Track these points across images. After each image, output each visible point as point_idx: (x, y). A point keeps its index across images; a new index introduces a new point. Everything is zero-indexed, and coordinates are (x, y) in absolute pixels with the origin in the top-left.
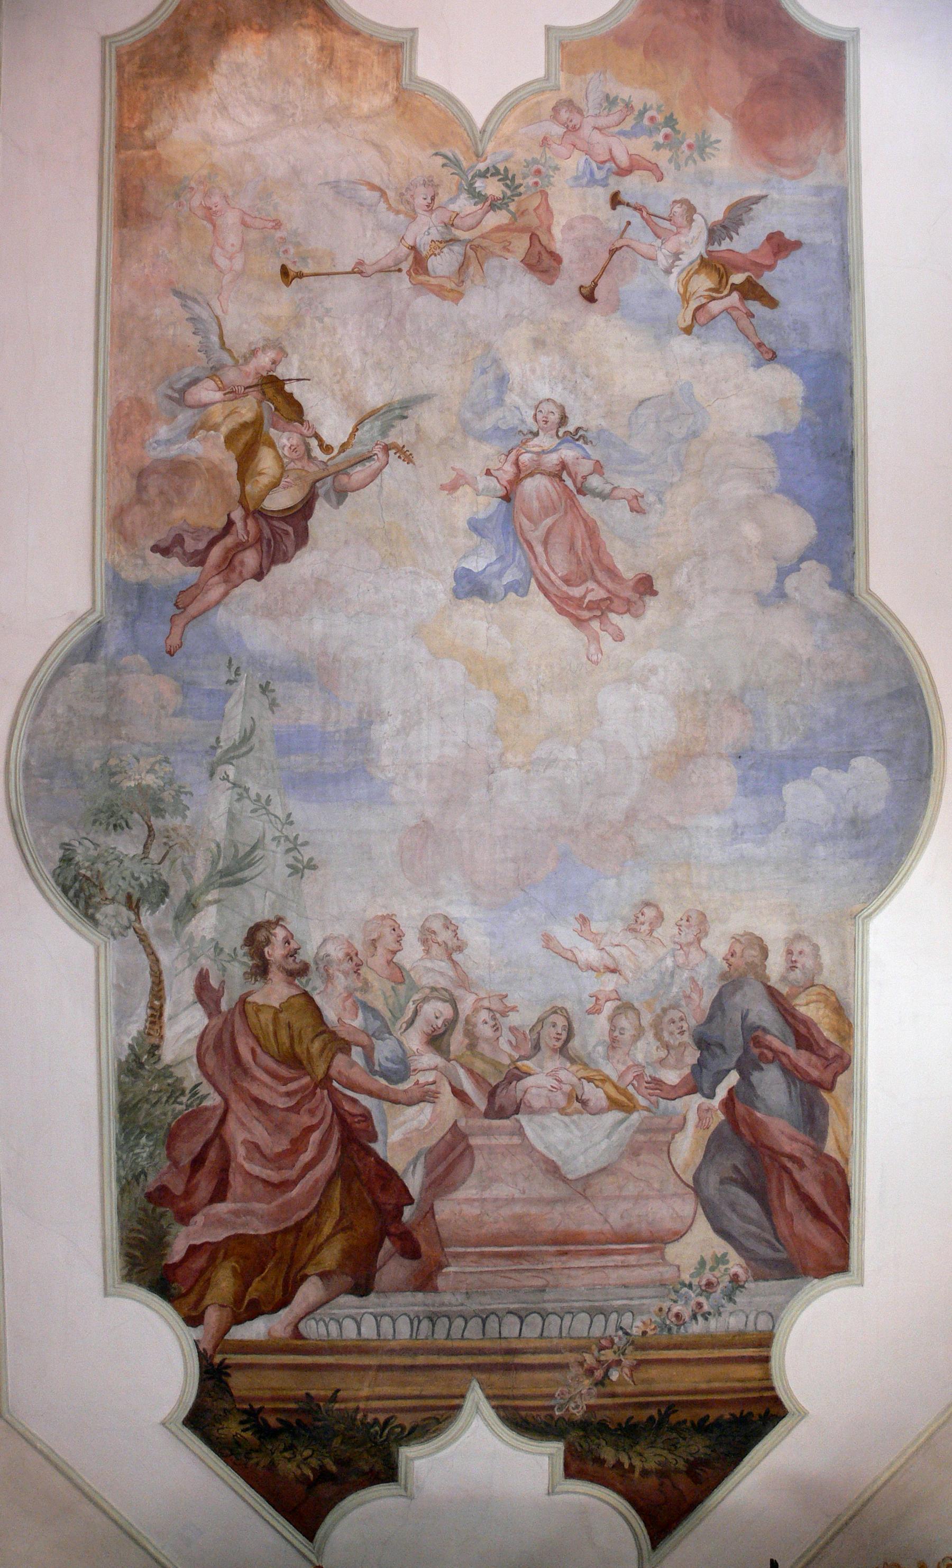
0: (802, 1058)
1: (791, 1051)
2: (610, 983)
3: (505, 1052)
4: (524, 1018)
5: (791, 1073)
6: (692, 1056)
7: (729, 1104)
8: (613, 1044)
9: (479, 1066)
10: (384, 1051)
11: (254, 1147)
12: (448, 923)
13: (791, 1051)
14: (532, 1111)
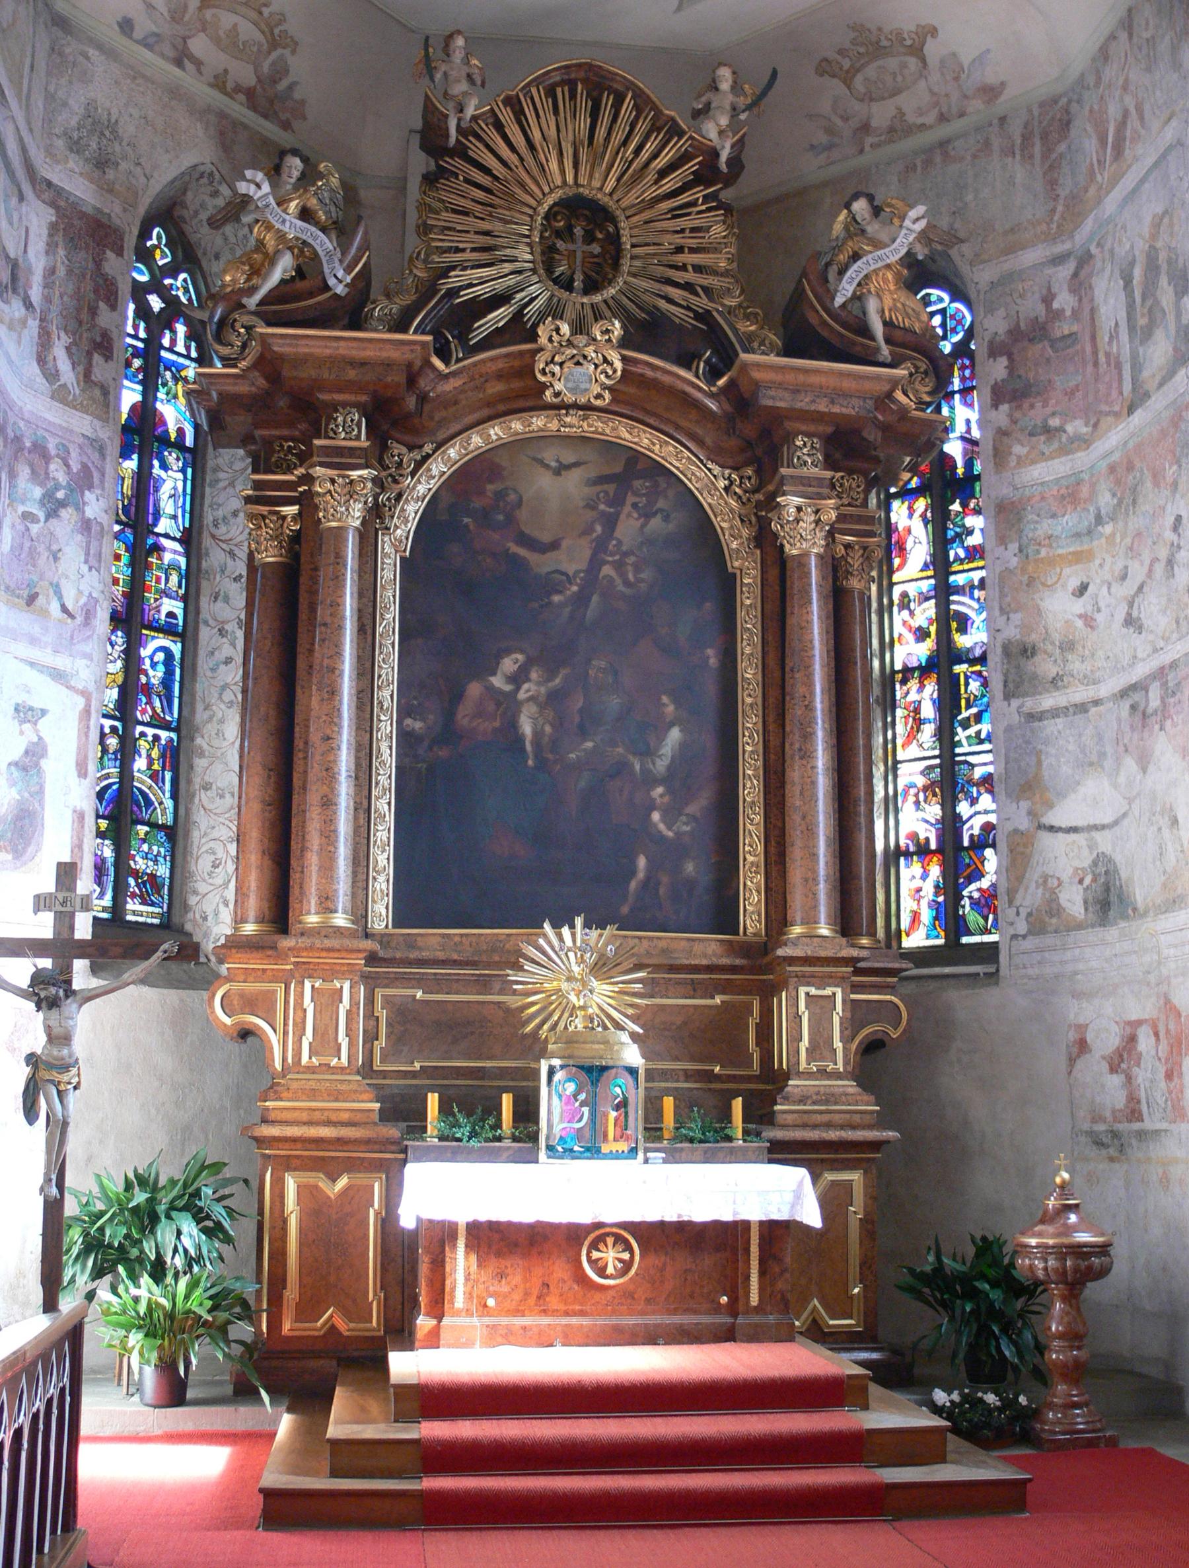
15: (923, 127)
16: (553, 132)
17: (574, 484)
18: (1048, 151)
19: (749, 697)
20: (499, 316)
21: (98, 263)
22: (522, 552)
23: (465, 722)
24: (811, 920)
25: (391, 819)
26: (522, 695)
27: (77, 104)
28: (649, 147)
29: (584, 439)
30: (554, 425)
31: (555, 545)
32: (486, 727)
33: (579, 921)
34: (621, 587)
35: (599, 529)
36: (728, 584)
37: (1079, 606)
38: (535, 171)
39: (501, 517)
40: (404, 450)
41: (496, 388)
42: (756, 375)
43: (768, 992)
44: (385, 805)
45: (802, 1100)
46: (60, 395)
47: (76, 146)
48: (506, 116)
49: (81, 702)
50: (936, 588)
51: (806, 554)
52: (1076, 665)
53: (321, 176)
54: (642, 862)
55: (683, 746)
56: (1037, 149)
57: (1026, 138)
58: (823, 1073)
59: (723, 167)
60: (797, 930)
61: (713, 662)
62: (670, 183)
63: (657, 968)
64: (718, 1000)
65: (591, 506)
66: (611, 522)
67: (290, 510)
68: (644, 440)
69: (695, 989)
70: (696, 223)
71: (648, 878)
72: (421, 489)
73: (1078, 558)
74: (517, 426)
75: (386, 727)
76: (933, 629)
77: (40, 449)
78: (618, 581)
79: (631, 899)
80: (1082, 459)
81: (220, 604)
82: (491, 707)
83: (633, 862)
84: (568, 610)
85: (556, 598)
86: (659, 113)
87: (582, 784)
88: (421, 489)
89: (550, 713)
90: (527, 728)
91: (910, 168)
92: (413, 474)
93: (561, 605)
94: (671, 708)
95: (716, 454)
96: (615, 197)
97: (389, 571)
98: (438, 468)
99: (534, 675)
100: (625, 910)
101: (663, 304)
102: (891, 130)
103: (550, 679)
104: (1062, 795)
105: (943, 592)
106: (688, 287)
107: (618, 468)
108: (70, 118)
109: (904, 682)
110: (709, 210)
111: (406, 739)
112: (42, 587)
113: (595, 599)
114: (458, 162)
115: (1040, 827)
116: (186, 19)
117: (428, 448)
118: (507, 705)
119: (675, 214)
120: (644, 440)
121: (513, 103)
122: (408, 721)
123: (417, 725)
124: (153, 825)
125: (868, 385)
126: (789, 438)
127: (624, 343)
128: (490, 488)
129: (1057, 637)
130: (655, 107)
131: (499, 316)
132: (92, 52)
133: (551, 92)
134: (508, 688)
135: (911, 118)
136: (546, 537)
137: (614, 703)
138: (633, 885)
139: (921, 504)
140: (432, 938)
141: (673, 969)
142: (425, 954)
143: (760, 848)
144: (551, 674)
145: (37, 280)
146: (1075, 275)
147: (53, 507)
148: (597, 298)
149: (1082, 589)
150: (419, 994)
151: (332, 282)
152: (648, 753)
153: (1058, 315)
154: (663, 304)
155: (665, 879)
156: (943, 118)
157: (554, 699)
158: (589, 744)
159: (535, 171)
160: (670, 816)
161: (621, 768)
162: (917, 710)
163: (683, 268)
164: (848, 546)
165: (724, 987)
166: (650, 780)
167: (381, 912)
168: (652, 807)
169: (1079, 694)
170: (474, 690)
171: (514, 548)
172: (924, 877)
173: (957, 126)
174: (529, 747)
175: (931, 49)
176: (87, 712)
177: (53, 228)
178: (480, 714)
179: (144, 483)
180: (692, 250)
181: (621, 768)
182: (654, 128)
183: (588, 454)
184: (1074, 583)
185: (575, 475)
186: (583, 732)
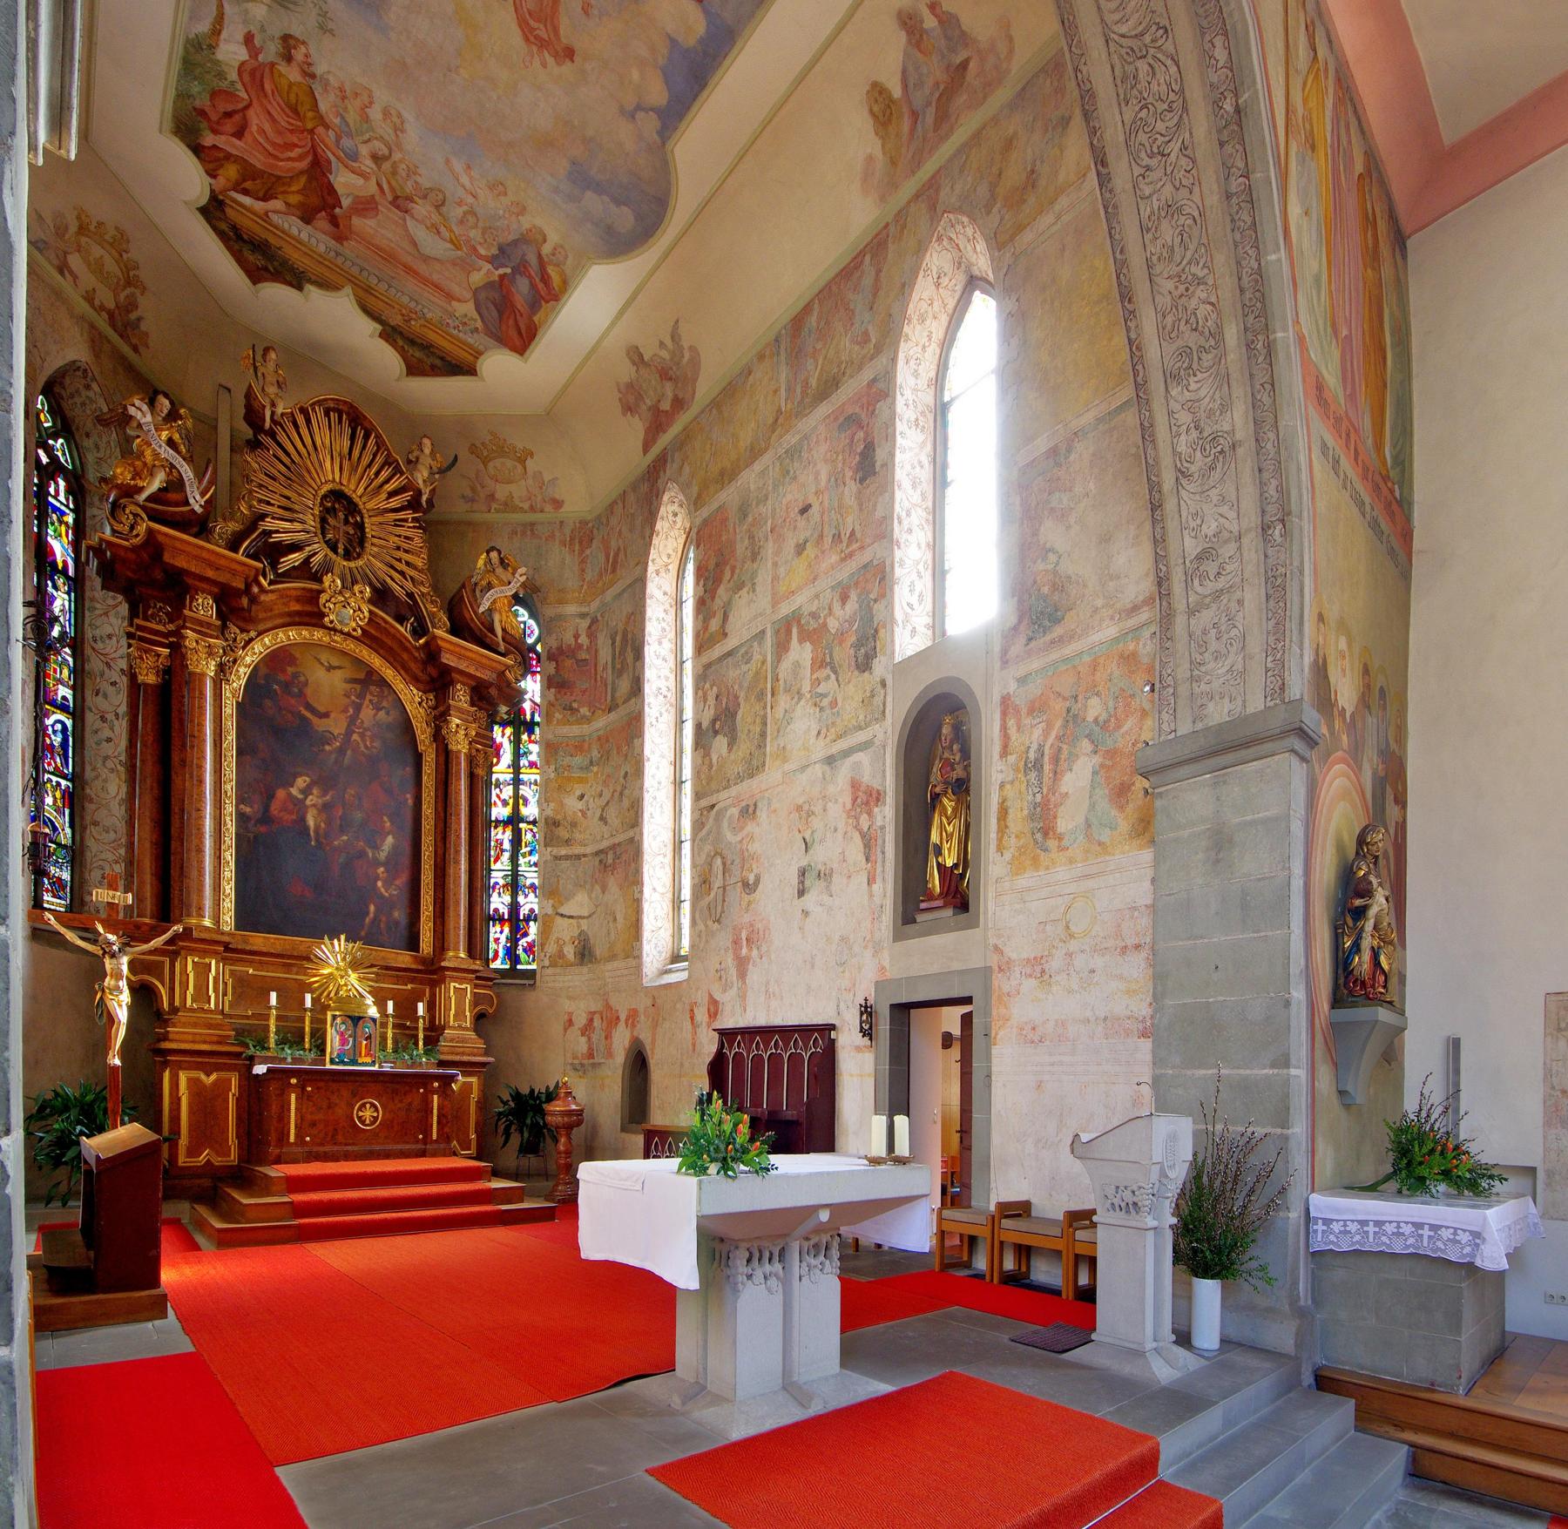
0: (541, 286)
1: (537, 280)
2: (470, 200)
3: (409, 188)
4: (426, 183)
5: (533, 286)
6: (495, 251)
7: (502, 277)
8: (461, 222)
9: (394, 183)
10: (346, 143)
11: (262, 131)
12: (399, 116)
13: (537, 280)
14: (412, 217)
18: (582, 551)
19: (428, 825)
20: (295, 558)
22: (308, 715)
23: (276, 812)
25: (232, 865)
26: (308, 802)
28: (384, 475)
30: (326, 639)
31: (326, 715)
32: (289, 818)
34: (363, 749)
35: (351, 710)
36: (418, 758)
37: (580, 805)
39: (296, 690)
40: (238, 631)
41: (296, 607)
43: (434, 984)
44: (229, 856)
48: (301, 419)
50: (513, 779)
51: (460, 751)
52: (577, 836)
53: (181, 418)
54: (372, 908)
56: (577, 548)
57: (572, 539)
60: (451, 954)
61: (410, 802)
62: (395, 502)
64: (409, 987)
65: (347, 696)
66: (358, 708)
67: (166, 651)
68: (376, 662)
69: (398, 980)
70: (408, 534)
72: (248, 660)
73: (581, 780)
75: (230, 808)
76: (511, 801)
78: (362, 745)
79: (366, 928)
80: (585, 729)
81: (100, 699)
83: (368, 907)
84: (333, 756)
85: (327, 748)
86: (389, 454)
87: (341, 860)
88: (248, 660)
90: (311, 822)
92: (244, 648)
93: (331, 752)
94: (388, 824)
95: (415, 680)
96: (364, 499)
97: (229, 709)
99: (315, 791)
100: (363, 934)
103: (324, 795)
104: (567, 899)
105: (517, 782)
106: (402, 573)
107: (362, 676)
109: (496, 827)
110: (414, 527)
111: (241, 818)
113: (349, 752)
114: (268, 440)
116: (67, 237)
117: (253, 634)
118: (299, 806)
119: (398, 523)
121: (303, 411)
122: (242, 806)
124: (59, 845)
126: (452, 683)
127: (371, 601)
128: (290, 670)
131: (295, 558)
134: (300, 796)
135: (517, 502)
136: (322, 709)
137: (358, 816)
138: (367, 920)
139: (509, 730)
140: (259, 941)
141: (387, 968)
142: (255, 948)
143: (431, 908)
144: (325, 793)
146: (589, 627)
148: (352, 564)
149: (582, 797)
150: (251, 971)
151: (192, 501)
152: (376, 848)
153: (580, 647)
155: (384, 919)
156: (532, 509)
157: (326, 808)
158: (345, 838)
160: (387, 884)
161: (362, 854)
162: (502, 844)
163: (399, 560)
164: (477, 750)
165: (412, 981)
168: (377, 878)
169: (577, 850)
170: (281, 794)
172: (501, 932)
174: (312, 833)
180: (406, 551)
183: (346, 663)
184: (578, 793)
185: (338, 676)
186: (342, 830)
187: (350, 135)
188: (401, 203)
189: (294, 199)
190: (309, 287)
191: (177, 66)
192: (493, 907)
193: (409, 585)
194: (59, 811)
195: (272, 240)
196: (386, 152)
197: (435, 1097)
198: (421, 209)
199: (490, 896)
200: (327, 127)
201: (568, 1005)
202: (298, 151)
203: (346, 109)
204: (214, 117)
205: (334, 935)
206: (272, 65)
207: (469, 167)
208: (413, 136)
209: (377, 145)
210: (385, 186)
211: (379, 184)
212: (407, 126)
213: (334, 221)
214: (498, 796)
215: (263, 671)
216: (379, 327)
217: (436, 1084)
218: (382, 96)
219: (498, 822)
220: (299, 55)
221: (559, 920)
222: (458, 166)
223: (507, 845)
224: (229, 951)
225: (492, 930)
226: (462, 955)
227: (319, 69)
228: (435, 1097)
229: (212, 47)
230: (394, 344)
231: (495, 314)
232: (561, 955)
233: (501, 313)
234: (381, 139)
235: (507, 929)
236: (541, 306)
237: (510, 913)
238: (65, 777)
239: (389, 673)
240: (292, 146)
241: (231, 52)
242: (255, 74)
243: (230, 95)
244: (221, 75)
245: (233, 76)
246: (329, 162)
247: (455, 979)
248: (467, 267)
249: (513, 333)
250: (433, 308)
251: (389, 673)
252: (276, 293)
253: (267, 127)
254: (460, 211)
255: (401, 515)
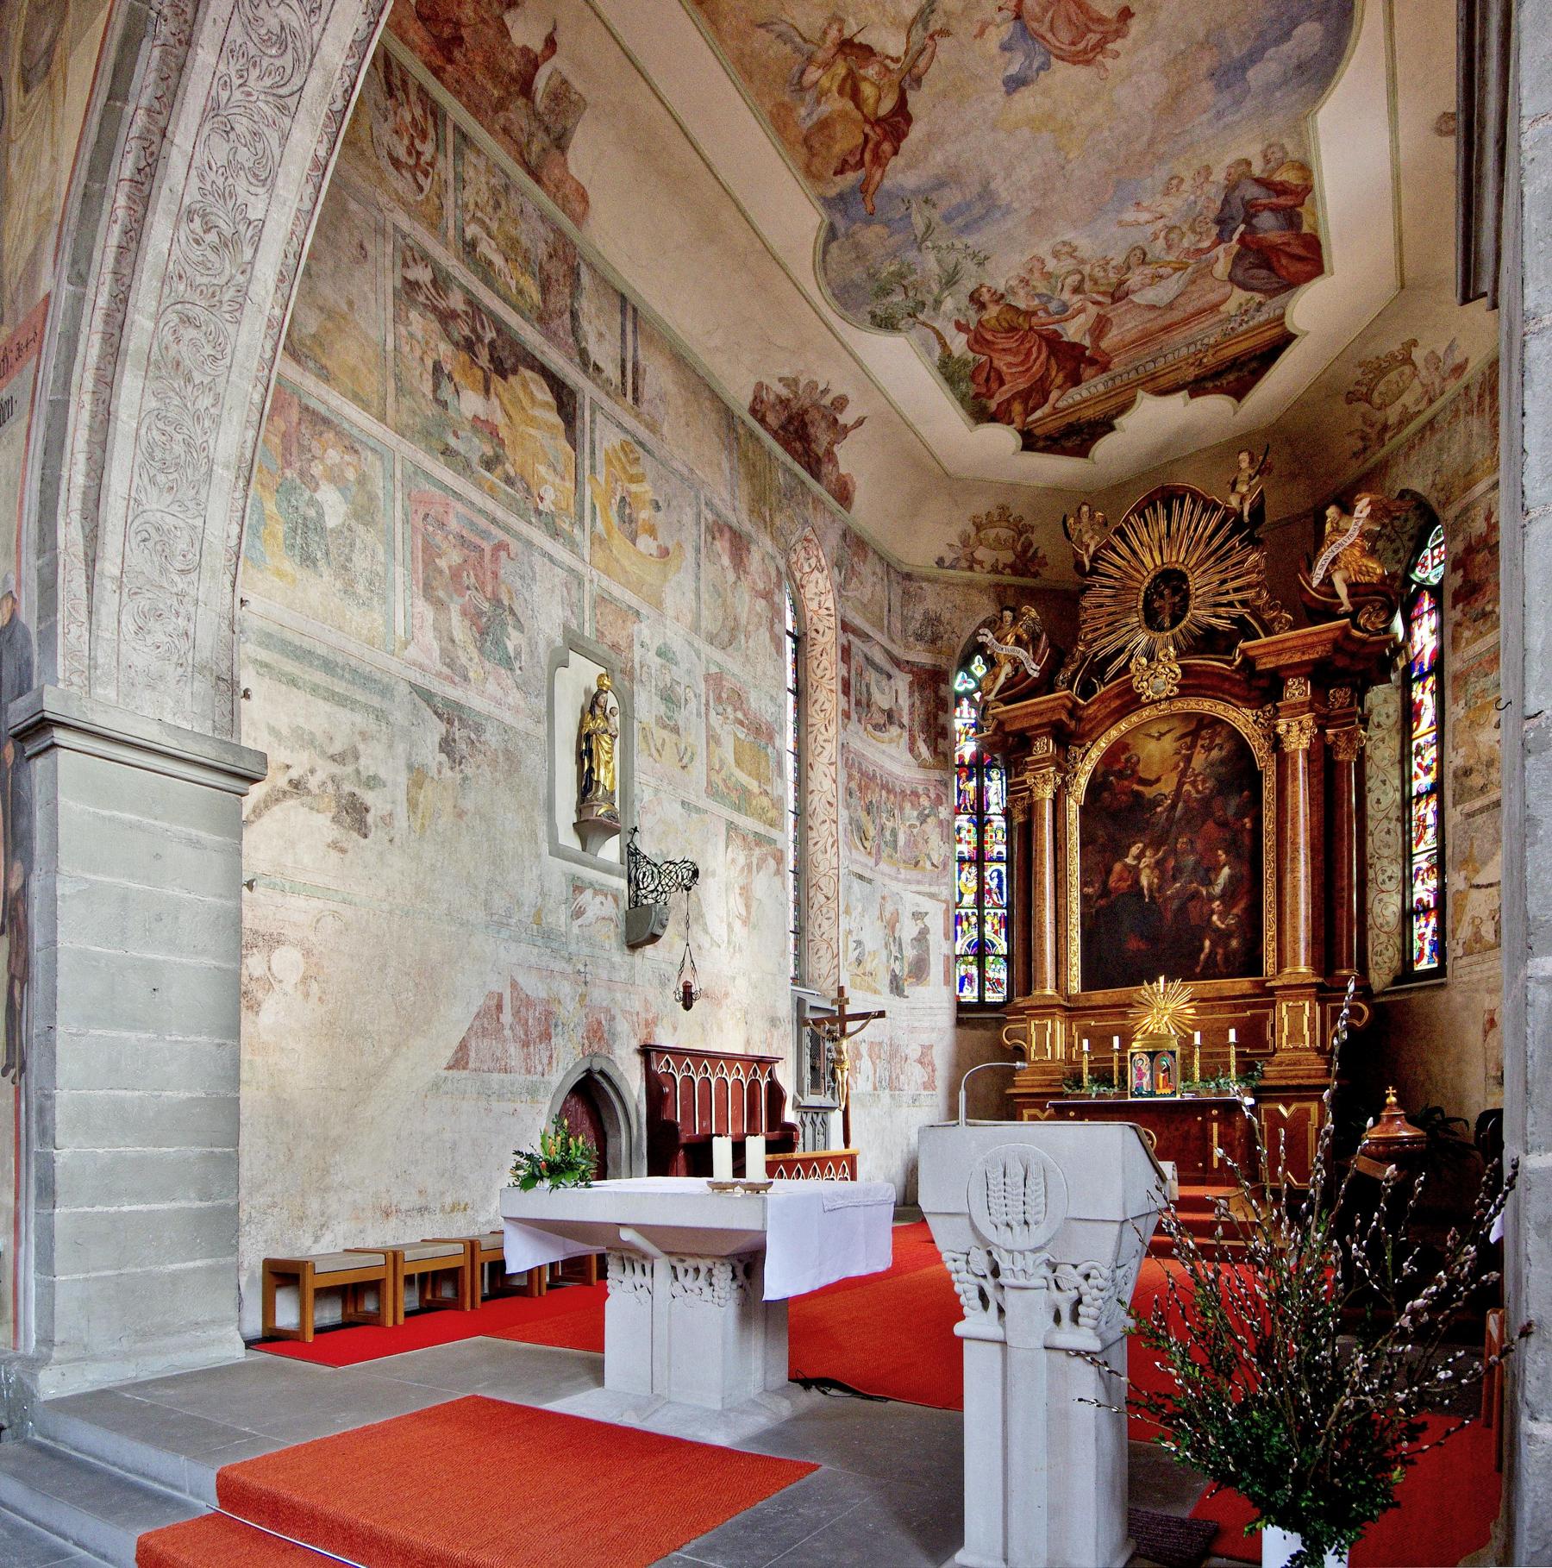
0: (1282, 201)
1: (1274, 200)
2: (1160, 224)
3: (1113, 277)
4: (1119, 260)
5: (1274, 209)
6: (1215, 230)
7: (1241, 240)
8: (1169, 247)
9: (1102, 289)
10: (1053, 307)
11: (1010, 365)
12: (1064, 243)
13: (1274, 200)
14: (1134, 292)
15: (1419, 412)
16: (1146, 538)
17: (1168, 743)
19: (1268, 842)
21: (936, 692)
22: (1140, 788)
24: (1296, 964)
27: (918, 616)
29: (1173, 716)
31: (1158, 780)
32: (1124, 885)
33: (1162, 979)
34: (1194, 795)
37: (1497, 735)
38: (1138, 566)
42: (1251, 653)
45: (1280, 1064)
46: (923, 765)
47: (919, 637)
49: (944, 906)
54: (1207, 943)
55: (1231, 877)
58: (1296, 1048)
59: (1246, 519)
60: (1287, 970)
62: (1216, 542)
63: (1203, 1000)
65: (1177, 753)
66: (1188, 759)
68: (1206, 706)
69: (1237, 1008)
71: (1211, 951)
74: (1134, 719)
77: (915, 794)
82: (1125, 875)
88: (1088, 768)
89: (1157, 872)
90: (1144, 882)
91: (1412, 447)
98: (1095, 754)
100: (1198, 970)
101: (1213, 621)
102: (1401, 422)
104: (1484, 863)
106: (1231, 604)
107: (1192, 727)
108: (914, 626)
111: (1085, 898)
112: (922, 857)
115: (1472, 886)
117: (1089, 744)
118: (1135, 872)
119: (1221, 559)
120: (1206, 706)
123: (1089, 890)
125: (1324, 636)
128: (1123, 758)
129: (1484, 758)
130: (1203, 498)
132: (924, 584)
133: (1142, 515)
136: (1153, 777)
141: (1222, 999)
145: (906, 712)
147: (923, 819)
154: (1213, 621)
155: (1220, 951)
156: (1431, 401)
157: (1159, 865)
159: (1138, 566)
160: (1223, 917)
166: (1211, 899)
167: (1075, 985)
168: (1213, 912)
170: (1118, 867)
171: (1136, 787)
173: (1437, 405)
175: (1418, 355)
176: (947, 910)
177: (911, 683)
178: (1121, 879)
179: (980, 791)
181: (1195, 895)
182: (1205, 510)
183: (1175, 723)
184: (1494, 721)
185: (1169, 736)
186: (1175, 879)
187: (1050, 299)
188: (1118, 294)
189: (1059, 380)
190: (1116, 422)
191: (946, 387)
192: (1415, 898)
193: (1240, 610)
194: (996, 932)
195: (1072, 419)
196: (1077, 277)
197: (1215, 1125)
198: (1134, 279)
199: (1412, 886)
200: (1034, 313)
201: (1488, 1002)
202: (1035, 349)
203: (1034, 287)
204: (984, 390)
205: (1152, 979)
206: (980, 322)
207: (1138, 204)
208: (1086, 245)
209: (1073, 280)
210: (1100, 298)
211: (1094, 303)
212: (1075, 243)
213: (1092, 362)
214: (1419, 765)
215: (1101, 769)
216: (1185, 393)
217: (1215, 1112)
218: (1043, 249)
219: (1419, 796)
220: (986, 297)
221: (1474, 893)
222: (1129, 216)
223: (1431, 819)
224: (1072, 1010)
225: (1416, 925)
226: (1303, 969)
227: (1001, 289)
228: (1215, 1125)
229: (950, 356)
230: (1206, 392)
231: (1264, 273)
232: (1477, 937)
233: (1270, 268)
234: (1069, 273)
235: (1433, 921)
236: (1299, 215)
237: (1436, 900)
238: (1001, 907)
239: (1219, 709)
240: (1029, 351)
241: (959, 343)
242: (978, 341)
243: (980, 367)
244: (966, 364)
245: (971, 355)
246: (1055, 331)
247: (1285, 998)
248: (1206, 271)
249: (1297, 267)
250: (1207, 331)
251: (1219, 709)
252: (1105, 447)
253: (1010, 359)
254: (1161, 242)
255: (1227, 547)
